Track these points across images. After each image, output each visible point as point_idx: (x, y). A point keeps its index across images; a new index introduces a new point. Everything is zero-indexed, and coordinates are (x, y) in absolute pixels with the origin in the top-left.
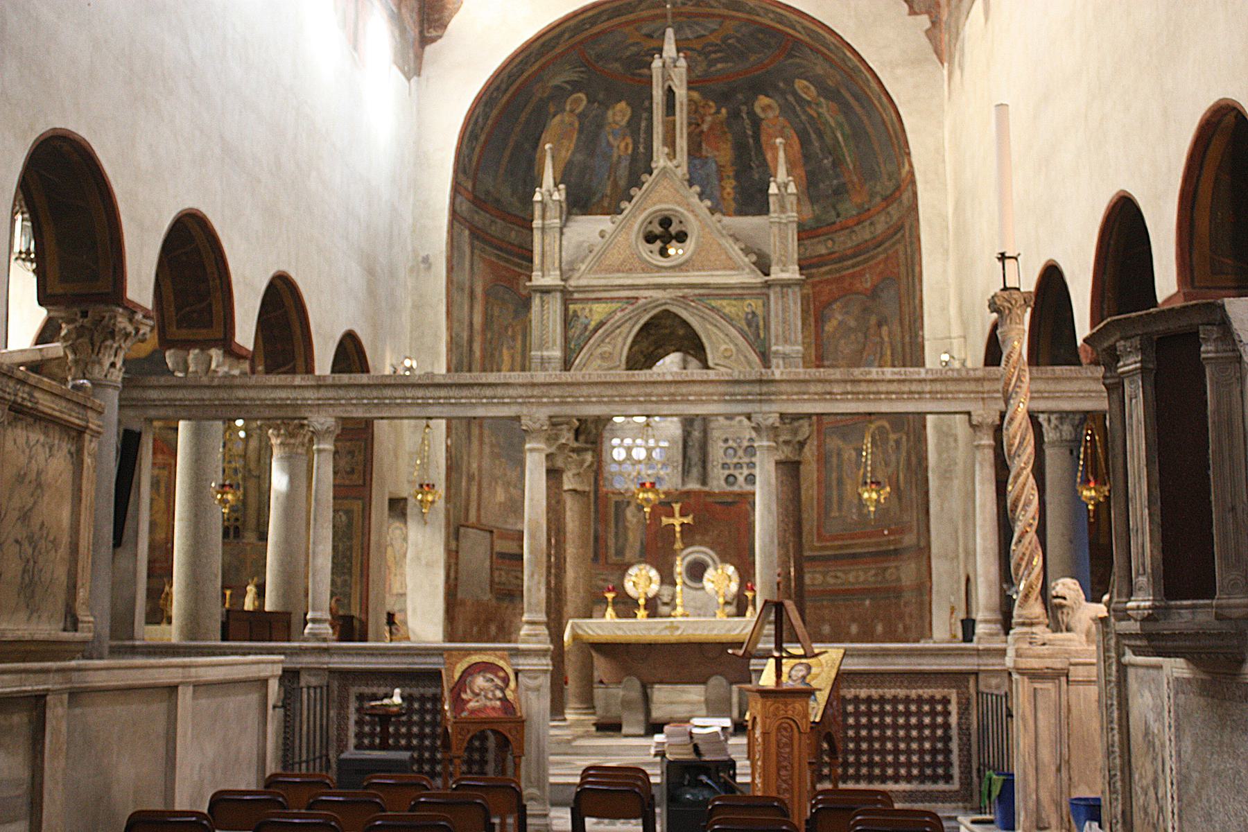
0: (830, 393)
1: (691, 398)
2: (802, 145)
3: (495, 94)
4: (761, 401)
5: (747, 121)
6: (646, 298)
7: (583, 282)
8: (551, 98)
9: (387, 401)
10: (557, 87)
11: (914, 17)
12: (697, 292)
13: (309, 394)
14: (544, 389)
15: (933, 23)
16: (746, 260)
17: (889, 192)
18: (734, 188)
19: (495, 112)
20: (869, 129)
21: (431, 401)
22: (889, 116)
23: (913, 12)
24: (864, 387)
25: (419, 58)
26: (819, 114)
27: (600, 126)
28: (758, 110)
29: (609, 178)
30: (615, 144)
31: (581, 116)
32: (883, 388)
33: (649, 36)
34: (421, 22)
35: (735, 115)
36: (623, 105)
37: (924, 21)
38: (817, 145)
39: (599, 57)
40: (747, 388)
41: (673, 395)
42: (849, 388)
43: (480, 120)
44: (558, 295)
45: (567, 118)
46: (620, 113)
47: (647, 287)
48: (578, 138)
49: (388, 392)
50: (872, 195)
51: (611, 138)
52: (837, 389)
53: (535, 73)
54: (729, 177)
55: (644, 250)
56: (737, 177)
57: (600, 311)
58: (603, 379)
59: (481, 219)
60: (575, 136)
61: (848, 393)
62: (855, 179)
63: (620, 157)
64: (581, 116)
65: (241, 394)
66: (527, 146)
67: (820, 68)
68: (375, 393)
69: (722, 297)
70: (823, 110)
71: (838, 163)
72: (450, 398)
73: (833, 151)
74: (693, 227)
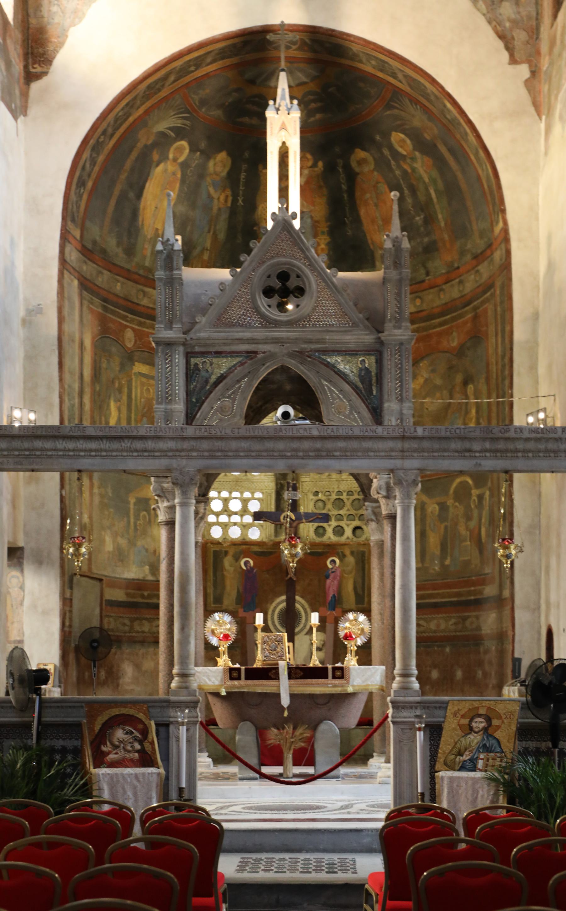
0: (470, 451)
1: (337, 454)
3: (101, 140)
4: (403, 458)
5: (342, 176)
6: (264, 353)
7: (203, 335)
9: (38, 453)
12: (313, 346)
14: (193, 443)
16: (361, 315)
17: (479, 251)
18: (328, 244)
21: (82, 454)
24: (501, 445)
29: (209, 232)
30: (215, 196)
31: (184, 166)
32: (520, 445)
40: (390, 444)
41: (318, 450)
42: (487, 445)
43: (88, 165)
44: (181, 349)
47: (266, 341)
48: (181, 190)
49: (38, 444)
50: (462, 253)
51: (211, 190)
52: (476, 446)
53: (140, 117)
54: (323, 233)
58: (252, 434)
60: (178, 185)
61: (486, 451)
62: (446, 237)
63: (219, 209)
66: (131, 195)
68: (26, 445)
69: (338, 352)
71: (430, 220)
72: (101, 450)
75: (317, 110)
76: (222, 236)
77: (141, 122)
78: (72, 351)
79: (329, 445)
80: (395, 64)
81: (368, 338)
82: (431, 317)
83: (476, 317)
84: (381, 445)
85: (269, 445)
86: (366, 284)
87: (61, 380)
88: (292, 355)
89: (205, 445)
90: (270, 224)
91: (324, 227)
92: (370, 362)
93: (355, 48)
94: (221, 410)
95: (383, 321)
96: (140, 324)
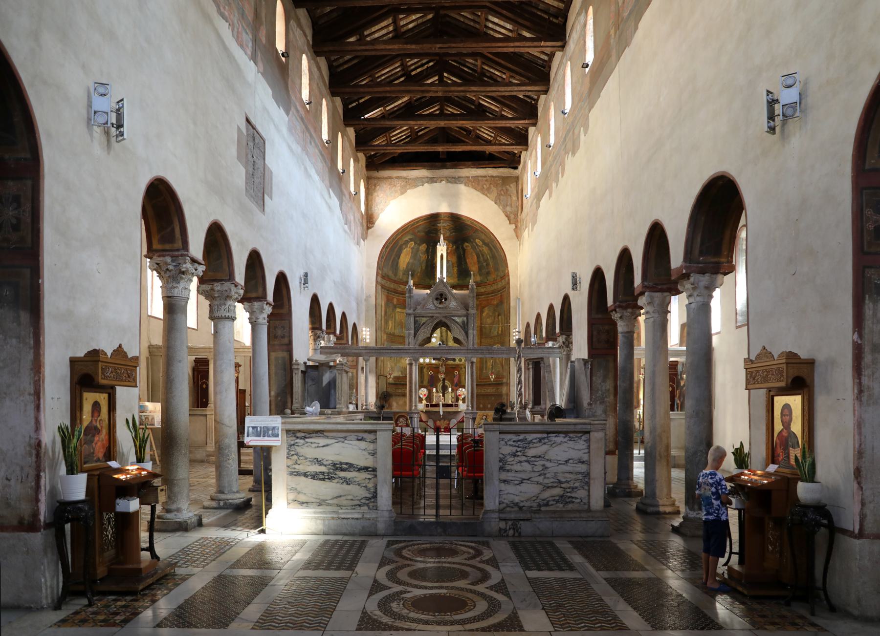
2: (477, 258)
8: (404, 244)
10: (406, 241)
11: (510, 226)
13: (363, 351)
15: (516, 227)
19: (388, 250)
20: (497, 256)
22: (503, 254)
23: (510, 223)
25: (367, 233)
26: (483, 250)
27: (418, 250)
28: (464, 246)
31: (412, 248)
33: (434, 225)
34: (367, 222)
35: (457, 248)
36: (425, 244)
37: (513, 226)
38: (482, 258)
39: (418, 231)
45: (408, 249)
46: (423, 247)
49: (381, 351)
50: (497, 276)
52: (485, 352)
55: (435, 302)
56: (458, 266)
57: (424, 320)
59: (384, 282)
64: (412, 248)
65: (347, 351)
67: (483, 237)
69: (457, 316)
70: (484, 249)
71: (488, 265)
73: (486, 261)
74: (449, 296)
75: (453, 232)
76: (424, 268)
77: (400, 238)
78: (379, 308)
79: (450, 351)
80: (476, 224)
81: (464, 312)
82: (489, 294)
83: (501, 296)
84: (462, 351)
85: (436, 351)
86: (464, 295)
87: (376, 317)
88: (443, 317)
89: (421, 351)
90: (438, 280)
91: (456, 265)
92: (465, 319)
93: (464, 219)
94: (424, 332)
95: (469, 307)
96: (399, 296)
